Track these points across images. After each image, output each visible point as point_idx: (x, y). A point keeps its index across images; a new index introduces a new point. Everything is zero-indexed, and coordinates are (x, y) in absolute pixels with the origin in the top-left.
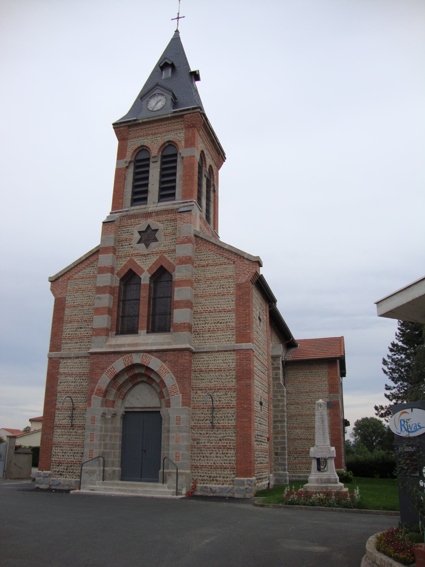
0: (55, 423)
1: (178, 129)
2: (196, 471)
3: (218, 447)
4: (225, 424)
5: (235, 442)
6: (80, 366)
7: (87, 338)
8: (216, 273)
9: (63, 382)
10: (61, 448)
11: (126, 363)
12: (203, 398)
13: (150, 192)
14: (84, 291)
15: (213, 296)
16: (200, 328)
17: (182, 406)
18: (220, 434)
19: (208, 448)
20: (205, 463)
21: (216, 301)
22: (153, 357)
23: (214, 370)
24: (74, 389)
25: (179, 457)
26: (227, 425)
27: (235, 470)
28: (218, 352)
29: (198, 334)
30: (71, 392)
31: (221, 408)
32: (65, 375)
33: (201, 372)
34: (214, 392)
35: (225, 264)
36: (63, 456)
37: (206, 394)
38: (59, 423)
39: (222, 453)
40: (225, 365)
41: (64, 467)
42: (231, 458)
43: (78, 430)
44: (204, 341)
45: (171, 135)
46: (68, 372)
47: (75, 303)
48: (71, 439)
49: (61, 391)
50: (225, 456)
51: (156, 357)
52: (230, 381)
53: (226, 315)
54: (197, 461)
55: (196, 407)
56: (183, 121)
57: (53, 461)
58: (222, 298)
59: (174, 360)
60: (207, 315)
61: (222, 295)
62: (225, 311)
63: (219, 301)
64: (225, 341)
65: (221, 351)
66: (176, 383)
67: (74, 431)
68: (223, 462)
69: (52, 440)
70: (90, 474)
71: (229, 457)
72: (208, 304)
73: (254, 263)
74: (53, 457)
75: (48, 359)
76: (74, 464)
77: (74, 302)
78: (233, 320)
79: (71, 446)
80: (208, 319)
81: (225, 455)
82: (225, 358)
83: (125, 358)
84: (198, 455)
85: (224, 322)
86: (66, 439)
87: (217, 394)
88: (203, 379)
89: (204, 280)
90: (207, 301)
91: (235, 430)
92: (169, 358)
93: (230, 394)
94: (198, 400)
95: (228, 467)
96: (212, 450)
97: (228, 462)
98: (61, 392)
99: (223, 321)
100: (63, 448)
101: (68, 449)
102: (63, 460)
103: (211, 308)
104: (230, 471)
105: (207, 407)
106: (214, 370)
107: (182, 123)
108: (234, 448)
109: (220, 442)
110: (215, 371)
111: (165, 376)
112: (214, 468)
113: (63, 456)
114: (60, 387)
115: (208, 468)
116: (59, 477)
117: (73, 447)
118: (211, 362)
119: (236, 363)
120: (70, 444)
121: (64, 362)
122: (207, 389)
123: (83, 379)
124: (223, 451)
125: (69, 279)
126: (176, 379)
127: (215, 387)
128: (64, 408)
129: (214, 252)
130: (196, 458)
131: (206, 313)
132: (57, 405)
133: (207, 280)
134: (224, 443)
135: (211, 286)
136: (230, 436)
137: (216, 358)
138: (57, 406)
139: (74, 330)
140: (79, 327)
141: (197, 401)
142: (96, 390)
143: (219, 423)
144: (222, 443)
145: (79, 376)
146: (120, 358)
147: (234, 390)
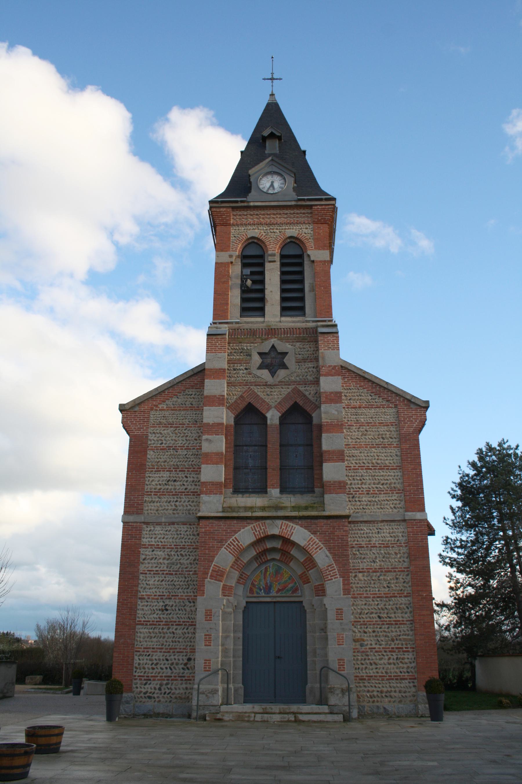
0: (137, 619)
1: (304, 223)
2: (361, 685)
3: (390, 649)
4: (398, 619)
5: (413, 642)
6: (176, 536)
7: (185, 495)
8: (372, 418)
9: (148, 559)
10: (150, 657)
11: (256, 534)
12: (364, 584)
13: (268, 301)
14: (178, 429)
15: (371, 447)
16: (355, 490)
17: (344, 595)
18: (392, 631)
19: (376, 652)
20: (374, 673)
21: (375, 454)
22: (297, 527)
23: (378, 545)
24: (168, 569)
25: (344, 665)
26: (401, 619)
27: (416, 681)
28: (382, 521)
29: (353, 497)
30: (163, 574)
31: (391, 597)
32: (151, 548)
33: (360, 549)
34: (381, 575)
35: (383, 408)
36: (153, 669)
37: (369, 578)
38: (144, 619)
39: (397, 658)
40: (393, 539)
41: (154, 685)
42: (409, 665)
43: (176, 629)
44: (361, 507)
45: (293, 229)
46: (158, 543)
47: (163, 445)
48: (165, 643)
49: (146, 572)
50: (401, 662)
51: (301, 527)
52: (401, 560)
53: (389, 473)
54: (362, 670)
55: (356, 596)
56: (311, 213)
57: (137, 677)
58: (382, 451)
59: (328, 531)
60: (362, 472)
61: (382, 447)
62: (388, 469)
63: (378, 454)
64: (391, 508)
65: (387, 521)
66: (333, 562)
67: (171, 630)
68: (397, 671)
69: (134, 644)
70: (208, 695)
71: (406, 663)
72: (364, 458)
73: (422, 409)
74: (136, 672)
75: (122, 524)
76: (172, 680)
77: (162, 443)
78: (399, 480)
79: (166, 654)
80: (365, 478)
81: (401, 660)
82: (391, 531)
83: (254, 526)
84: (363, 662)
85: (387, 483)
86: (156, 643)
87: (384, 579)
88: (364, 558)
89: (356, 426)
90: (362, 454)
91: (412, 627)
92: (321, 529)
93: (403, 579)
94: (358, 585)
95: (406, 677)
96: (383, 655)
97: (405, 670)
98: (146, 574)
99: (386, 482)
100: (152, 656)
101: (161, 658)
102: (153, 675)
103: (368, 463)
104: (409, 682)
105: (372, 596)
106: (378, 545)
107: (309, 215)
108: (413, 651)
109: (393, 643)
110: (380, 547)
111: (316, 553)
112: (387, 679)
113: (153, 669)
114: (143, 566)
115: (378, 680)
116: (148, 701)
117: (170, 656)
118: (374, 535)
119: (408, 537)
120: (164, 650)
121: (149, 529)
122: (371, 571)
123: (182, 555)
124: (397, 655)
125: (152, 409)
126: (333, 558)
127: (382, 569)
128: (153, 597)
129: (368, 390)
130: (361, 666)
131: (362, 469)
132: (140, 592)
133: (360, 426)
134: (398, 644)
135: (365, 435)
136: (405, 635)
137: (380, 530)
138: (139, 594)
139: (164, 483)
140: (171, 479)
141: (357, 587)
142: (210, 571)
143: (390, 618)
144: (395, 644)
145: (176, 550)
146: (247, 526)
147: (407, 573)
